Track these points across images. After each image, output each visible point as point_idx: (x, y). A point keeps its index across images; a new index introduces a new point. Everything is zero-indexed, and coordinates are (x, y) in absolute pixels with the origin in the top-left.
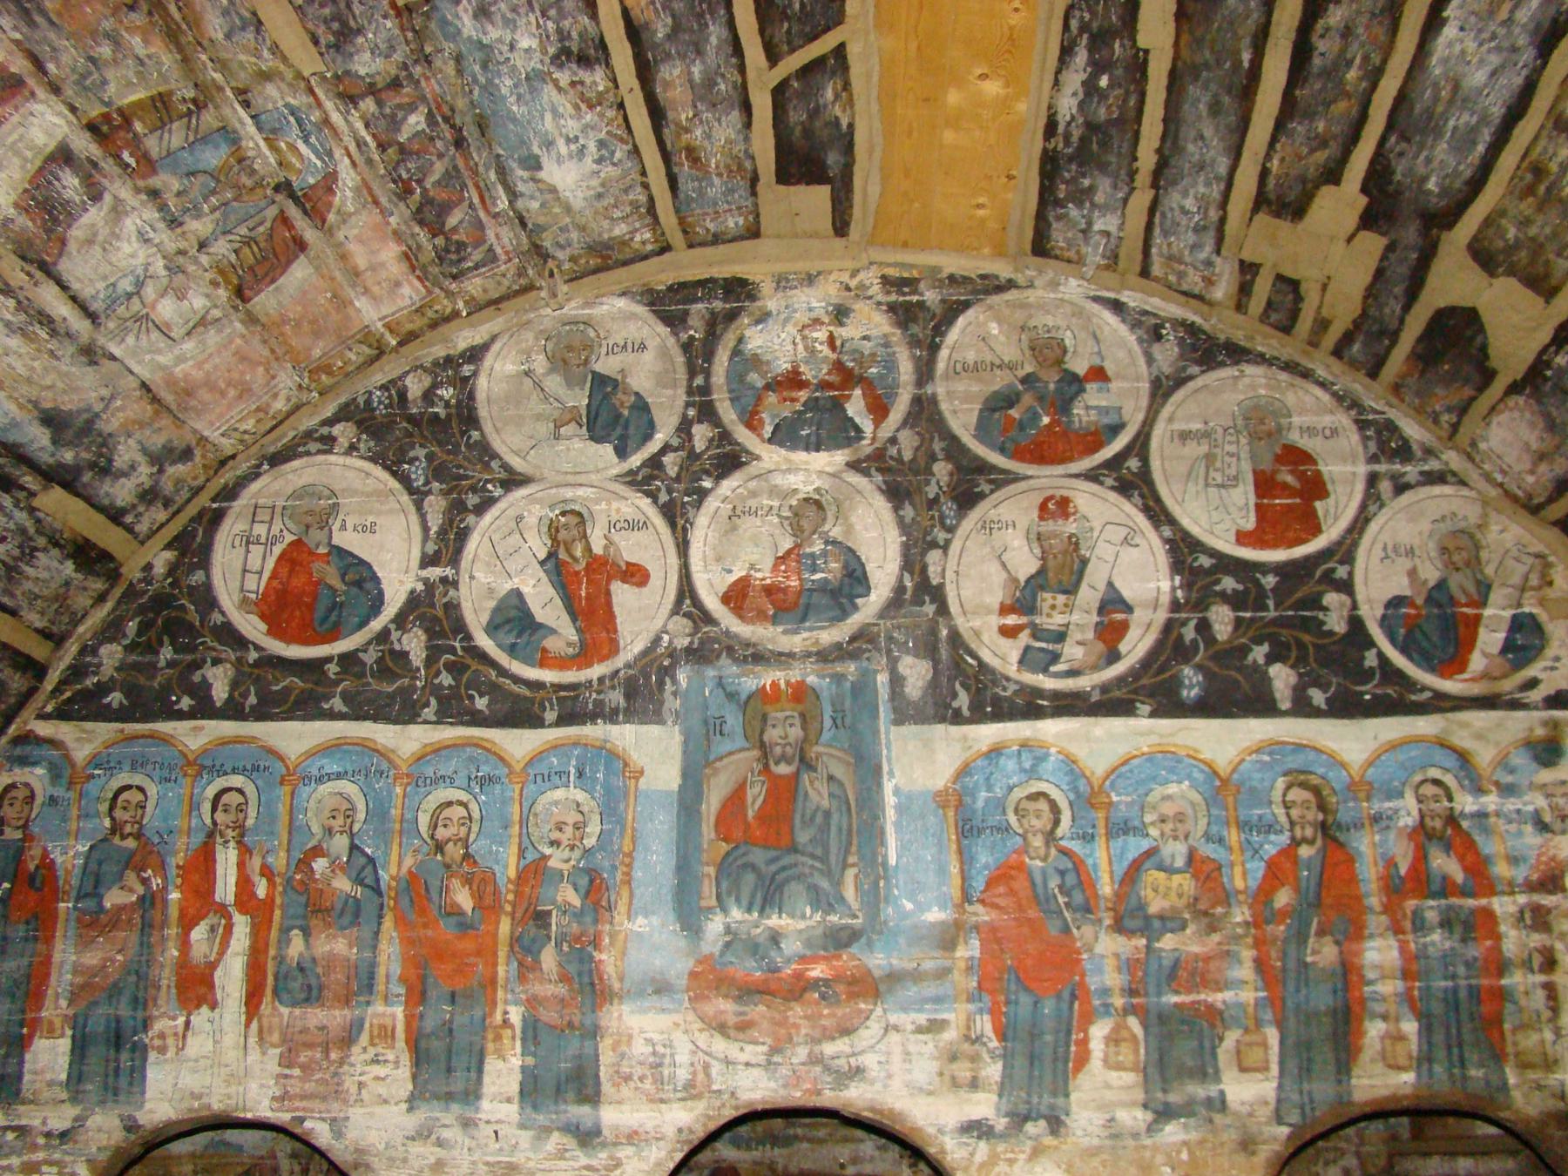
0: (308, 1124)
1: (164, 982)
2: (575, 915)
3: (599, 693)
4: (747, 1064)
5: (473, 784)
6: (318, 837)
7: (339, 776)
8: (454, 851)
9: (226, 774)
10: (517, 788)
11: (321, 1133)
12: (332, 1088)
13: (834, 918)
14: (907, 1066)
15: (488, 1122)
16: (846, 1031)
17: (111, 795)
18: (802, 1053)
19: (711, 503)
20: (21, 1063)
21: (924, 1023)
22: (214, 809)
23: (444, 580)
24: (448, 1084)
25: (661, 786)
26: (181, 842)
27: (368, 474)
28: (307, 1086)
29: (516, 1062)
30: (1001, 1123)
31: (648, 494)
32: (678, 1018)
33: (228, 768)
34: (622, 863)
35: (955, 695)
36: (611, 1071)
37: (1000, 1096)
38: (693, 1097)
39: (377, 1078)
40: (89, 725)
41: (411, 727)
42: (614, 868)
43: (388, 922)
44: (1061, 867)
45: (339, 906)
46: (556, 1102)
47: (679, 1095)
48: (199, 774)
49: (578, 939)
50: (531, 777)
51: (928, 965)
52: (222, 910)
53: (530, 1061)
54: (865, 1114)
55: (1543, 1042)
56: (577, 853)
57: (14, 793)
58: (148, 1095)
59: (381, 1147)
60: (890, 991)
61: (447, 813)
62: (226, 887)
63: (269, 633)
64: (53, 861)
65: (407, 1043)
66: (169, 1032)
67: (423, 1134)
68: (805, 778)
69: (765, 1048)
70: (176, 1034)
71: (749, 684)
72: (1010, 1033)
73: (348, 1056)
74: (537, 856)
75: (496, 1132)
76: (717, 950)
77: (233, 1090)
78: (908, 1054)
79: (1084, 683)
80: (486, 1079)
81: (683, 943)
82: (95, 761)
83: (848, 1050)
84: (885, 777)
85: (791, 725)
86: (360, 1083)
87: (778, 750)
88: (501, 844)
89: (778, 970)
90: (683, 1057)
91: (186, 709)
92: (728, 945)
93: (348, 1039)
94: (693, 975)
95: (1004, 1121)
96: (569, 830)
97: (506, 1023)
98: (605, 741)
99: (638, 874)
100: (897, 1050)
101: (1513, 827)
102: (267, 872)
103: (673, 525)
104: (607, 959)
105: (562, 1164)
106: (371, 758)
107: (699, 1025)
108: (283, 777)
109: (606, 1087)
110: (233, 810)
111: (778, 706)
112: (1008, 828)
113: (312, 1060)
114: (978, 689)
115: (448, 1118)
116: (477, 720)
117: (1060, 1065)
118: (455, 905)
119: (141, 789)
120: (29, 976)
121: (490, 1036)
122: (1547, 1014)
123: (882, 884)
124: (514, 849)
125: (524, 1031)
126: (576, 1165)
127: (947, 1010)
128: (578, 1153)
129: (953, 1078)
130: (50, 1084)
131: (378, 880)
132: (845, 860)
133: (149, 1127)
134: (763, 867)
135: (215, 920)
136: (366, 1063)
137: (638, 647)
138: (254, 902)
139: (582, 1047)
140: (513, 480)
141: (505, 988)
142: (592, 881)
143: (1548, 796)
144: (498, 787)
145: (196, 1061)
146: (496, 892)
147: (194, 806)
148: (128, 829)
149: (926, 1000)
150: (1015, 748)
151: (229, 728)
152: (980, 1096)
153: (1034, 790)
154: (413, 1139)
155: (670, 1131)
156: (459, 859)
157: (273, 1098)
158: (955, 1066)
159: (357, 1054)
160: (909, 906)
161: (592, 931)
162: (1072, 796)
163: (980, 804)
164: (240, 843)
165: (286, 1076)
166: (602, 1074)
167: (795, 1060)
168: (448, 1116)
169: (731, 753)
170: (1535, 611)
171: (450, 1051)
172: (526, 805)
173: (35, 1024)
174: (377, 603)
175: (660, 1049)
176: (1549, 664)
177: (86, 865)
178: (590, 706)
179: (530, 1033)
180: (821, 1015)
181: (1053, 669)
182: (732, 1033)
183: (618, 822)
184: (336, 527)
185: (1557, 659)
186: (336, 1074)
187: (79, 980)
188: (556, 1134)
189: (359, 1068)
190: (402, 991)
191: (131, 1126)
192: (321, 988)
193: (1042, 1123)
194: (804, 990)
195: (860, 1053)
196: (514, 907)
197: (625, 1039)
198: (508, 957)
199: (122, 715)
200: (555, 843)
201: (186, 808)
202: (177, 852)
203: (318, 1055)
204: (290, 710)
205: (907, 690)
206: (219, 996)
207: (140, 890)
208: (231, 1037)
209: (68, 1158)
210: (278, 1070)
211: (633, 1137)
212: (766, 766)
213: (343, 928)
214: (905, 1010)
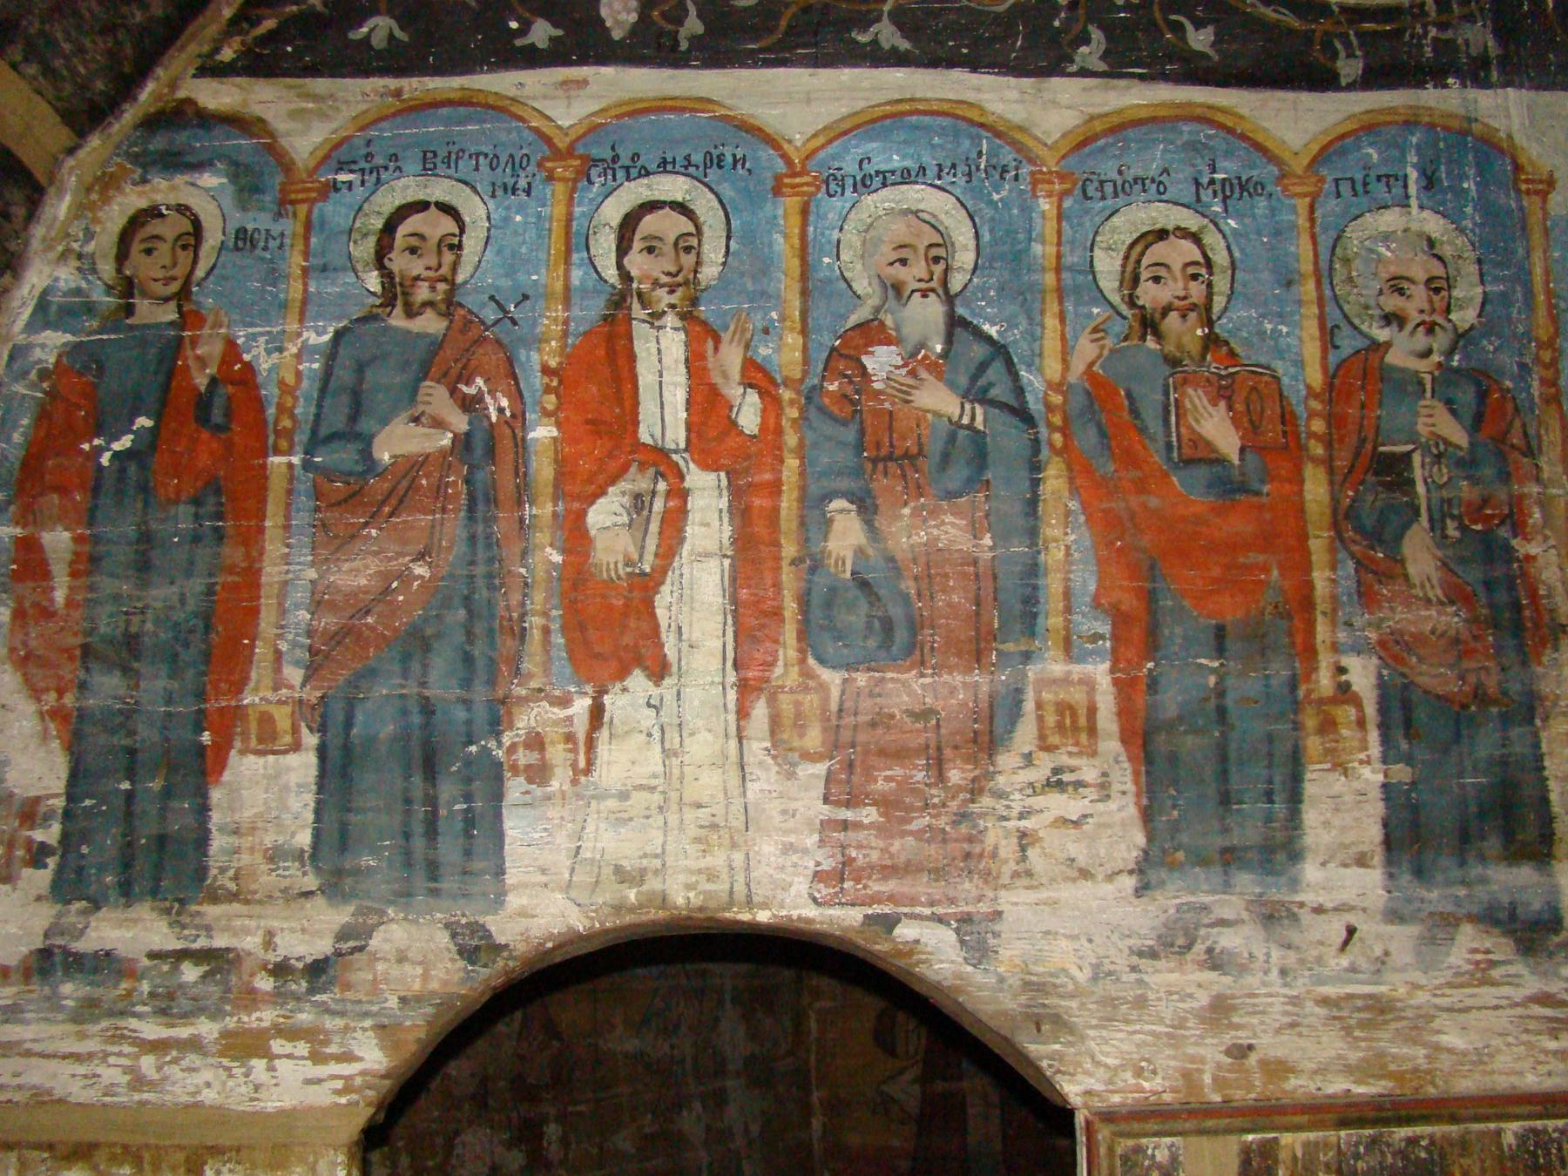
0: (906, 932)
1: (535, 621)
2: (1459, 463)
3: (1442, 26)
5: (1206, 196)
6: (875, 301)
7: (906, 177)
8: (1184, 332)
9: (648, 174)
10: (1302, 204)
12: (956, 848)
15: (1319, 910)
17: (378, 224)
20: (204, 809)
22: (623, 248)
24: (1226, 830)
26: (549, 320)
28: (896, 845)
29: (1372, 776)
33: (650, 160)
39: (1063, 822)
40: (321, 85)
41: (1056, 82)
43: (1054, 480)
45: (935, 448)
46: (1462, 864)
48: (584, 174)
49: (1477, 510)
50: (1328, 186)
52: (658, 459)
53: (1402, 773)
56: (1441, 341)
57: (155, 227)
58: (511, 878)
59: (1082, 976)
61: (1158, 251)
64: (249, 368)
65: (1124, 741)
66: (552, 733)
70: (570, 738)
73: (989, 776)
74: (1360, 343)
75: (1351, 931)
77: (717, 860)
80: (1311, 816)
82: (337, 155)
86: (1023, 835)
88: (1282, 317)
91: (542, 44)
96: (1419, 294)
97: (1344, 692)
98: (1470, 120)
102: (757, 376)
105: (1488, 994)
106: (976, 140)
108: (778, 178)
110: (668, 248)
113: (905, 785)
115: (1230, 906)
116: (1197, 72)
118: (1198, 441)
119: (448, 209)
120: (207, 619)
121: (1310, 721)
124: (1312, 327)
125: (1383, 709)
126: (1519, 994)
128: (1519, 968)
130: (275, 855)
131: (1020, 391)
133: (521, 948)
135: (643, 484)
136: (1033, 789)
138: (731, 442)
141: (1332, 616)
142: (1482, 396)
144: (1262, 204)
145: (624, 796)
146: (1287, 417)
147: (575, 241)
148: (422, 293)
154: (1153, 955)
156: (1194, 348)
157: (818, 876)
161: (1502, 495)
165: (845, 825)
171: (1223, 758)
172: (1325, 242)
173: (228, 724)
177: (328, 372)
178: (1428, 51)
179: (1397, 715)
186: (962, 816)
187: (328, 621)
188: (1467, 929)
189: (1017, 802)
190: (1105, 628)
192: (914, 626)
196: (1329, 445)
198: (1332, 550)
199: (396, 62)
200: (1392, 319)
201: (557, 244)
202: (541, 340)
203: (920, 776)
204: (781, 46)
206: (670, 650)
207: (461, 423)
208: (703, 744)
209: (331, 1023)
210: (826, 811)
213: (951, 495)
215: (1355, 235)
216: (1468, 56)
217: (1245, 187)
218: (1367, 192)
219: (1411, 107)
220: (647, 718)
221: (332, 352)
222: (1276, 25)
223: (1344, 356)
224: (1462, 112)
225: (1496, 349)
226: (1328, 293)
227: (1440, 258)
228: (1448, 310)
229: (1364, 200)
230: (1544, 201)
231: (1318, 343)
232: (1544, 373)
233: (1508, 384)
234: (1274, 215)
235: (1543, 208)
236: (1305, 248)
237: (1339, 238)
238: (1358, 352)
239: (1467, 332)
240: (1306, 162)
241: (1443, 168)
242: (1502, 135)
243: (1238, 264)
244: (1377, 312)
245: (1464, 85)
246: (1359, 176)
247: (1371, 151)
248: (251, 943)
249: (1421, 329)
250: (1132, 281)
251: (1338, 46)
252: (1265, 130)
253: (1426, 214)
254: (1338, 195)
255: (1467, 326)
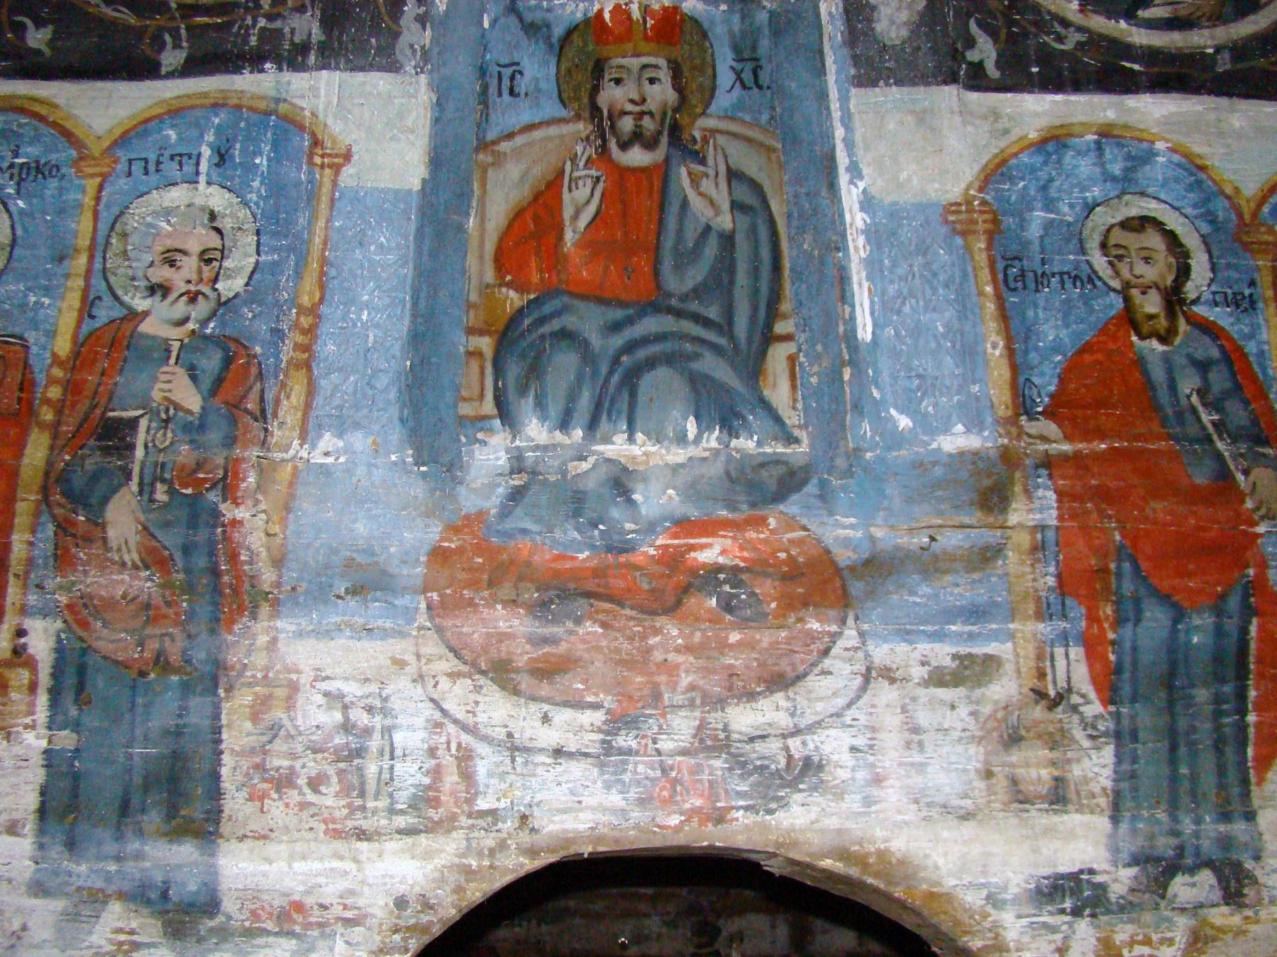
2: (187, 428)
3: (270, 17)
4: (558, 752)
13: (746, 444)
14: (917, 758)
16: (779, 681)
18: (682, 727)
21: (947, 662)
25: (386, 181)
29: (35, 742)
30: (1121, 880)
32: (401, 648)
34: (296, 326)
35: (971, 43)
36: (245, 764)
37: (1115, 819)
38: (432, 828)
42: (278, 333)
44: (1200, 354)
46: (119, 837)
47: (401, 821)
49: (189, 475)
50: (121, 167)
51: (952, 540)
53: (67, 740)
54: (827, 863)
56: (203, 308)
60: (871, 594)
68: (682, 174)
69: (598, 717)
72: (1126, 690)
74: (118, 312)
76: (492, 504)
78: (916, 730)
79: (1202, 39)
81: (419, 490)
83: (784, 720)
84: (843, 178)
85: (652, 81)
87: (627, 124)
88: (47, 290)
89: (628, 548)
90: (411, 737)
92: (516, 495)
94: (439, 555)
95: (1127, 874)
96: (189, 265)
99: (327, 348)
100: (892, 720)
107: (451, 664)
109: (235, 803)
111: (629, 47)
112: (1093, 277)
114: (1011, 35)
117: (1229, 751)
123: (847, 374)
124: (74, 299)
125: (58, 672)
127: (994, 636)
129: (1014, 782)
132: (769, 325)
134: (596, 341)
139: (182, 712)
141: (24, 578)
142: (228, 361)
144: (53, 184)
146: (27, 385)
149: (952, 614)
150: (1091, 137)
152: (1073, 820)
153: (1133, 212)
155: (378, 905)
158: (1015, 757)
160: (904, 422)
161: (220, 461)
162: (1205, 228)
163: (1034, 231)
166: (224, 771)
167: (666, 745)
169: (530, 128)
175: (360, 717)
178: (253, 41)
179: (70, 680)
180: (724, 646)
181: (1140, 13)
182: (525, 682)
183: (291, 249)
188: (116, 907)
193: (1206, 877)
194: (686, 589)
195: (812, 728)
196: (59, 413)
197: (281, 693)
198: (37, 514)
200: (159, 290)
205: (879, 27)
212: (604, 149)
214: (907, 635)
215: (139, 211)
216: (292, 43)
217: (39, 170)
218: (158, 171)
219: (223, 91)
222: (114, 22)
223: (97, 325)
224: (273, 93)
225: (254, 317)
226: (98, 265)
227: (219, 231)
228: (216, 280)
229: (153, 179)
230: (337, 173)
231: (75, 314)
232: (300, 339)
233: (258, 350)
234: (60, 196)
235: (335, 183)
236: (86, 224)
237: (122, 213)
238: (112, 321)
239: (229, 300)
240: (106, 144)
241: (238, 146)
242: (307, 113)
243: (19, 241)
244: (143, 283)
245: (280, 69)
246: (152, 157)
247: (171, 132)
249: (185, 298)
251: (168, 38)
252: (76, 117)
253: (213, 189)
254: (130, 174)
255: (231, 295)
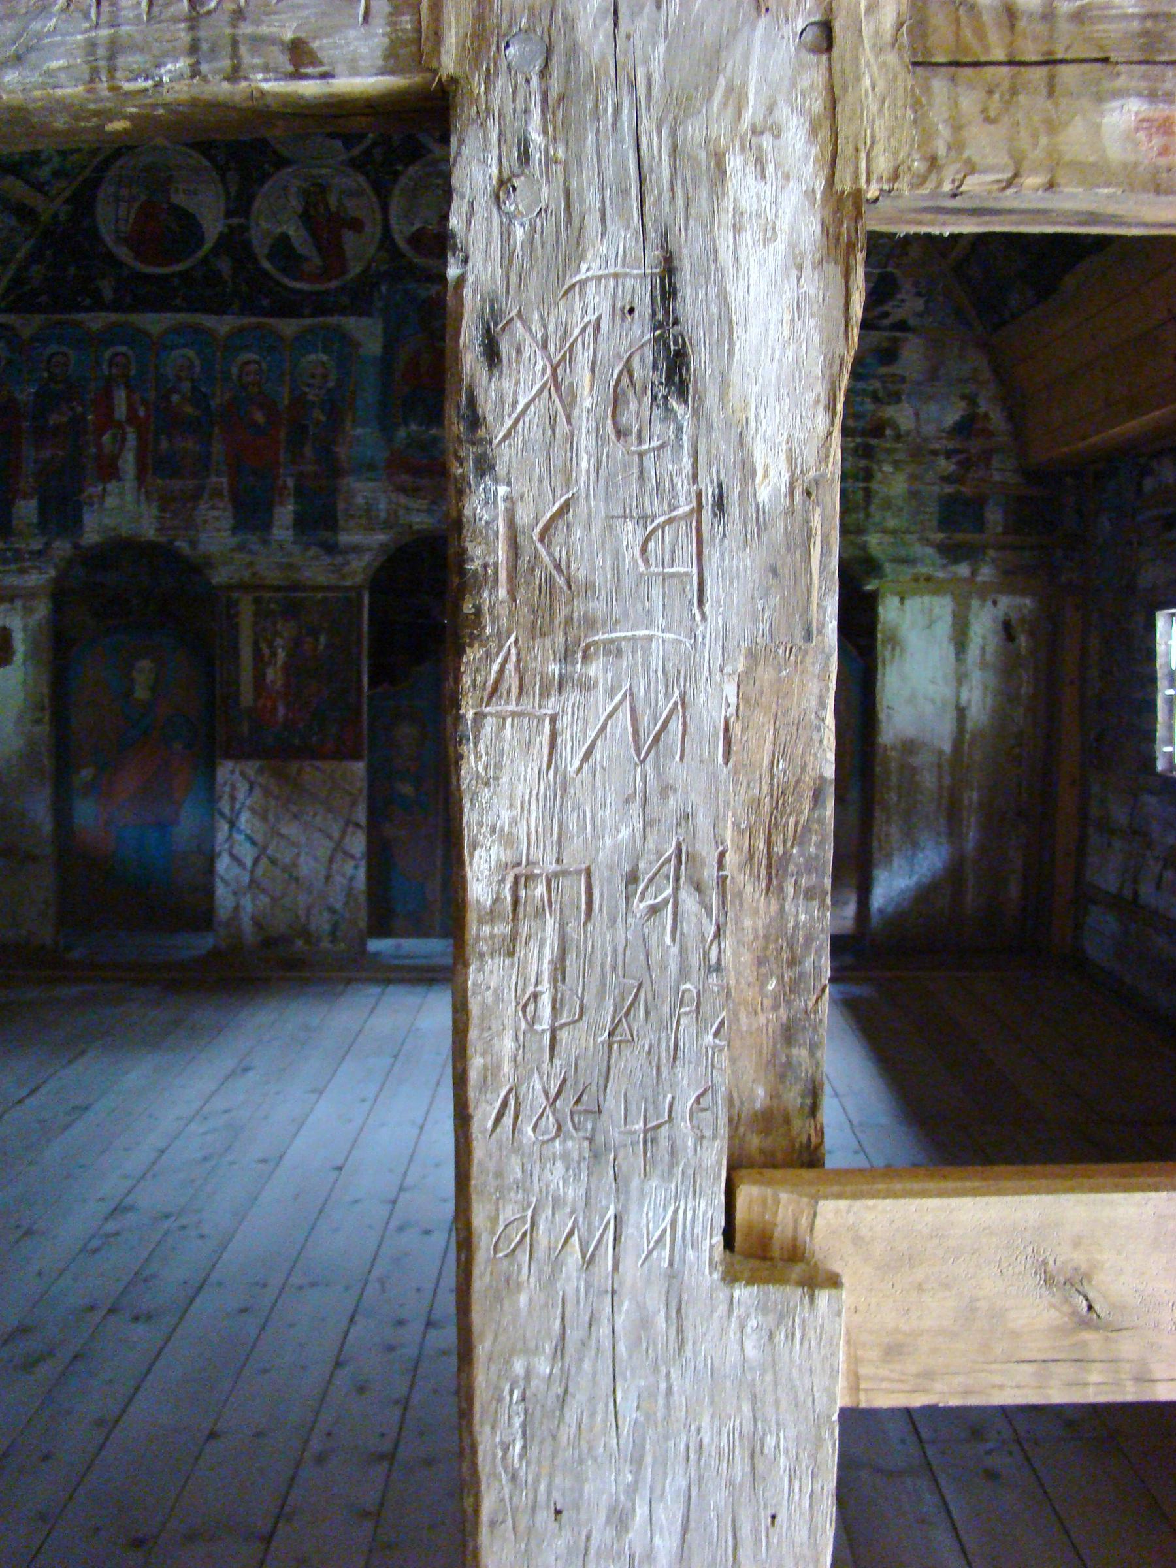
4: (418, 510)
7: (185, 346)
11: (182, 545)
19: (403, 181)
22: (110, 366)
23: (241, 226)
27: (190, 156)
29: (291, 508)
31: (362, 173)
41: (225, 317)
43: (216, 430)
52: (120, 425)
55: (858, 519)
56: (323, 391)
62: (121, 411)
63: (136, 259)
67: (241, 548)
71: (423, 294)
93: (196, 496)
97: (285, 487)
101: (858, 399)
102: (144, 402)
103: (378, 195)
104: (342, 452)
109: (341, 523)
115: (254, 538)
122: (862, 503)
130: (29, 525)
136: (208, 509)
137: (358, 270)
140: (282, 162)
143: (883, 382)
151: (114, 317)
155: (375, 546)
159: (203, 506)
164: (127, 387)
168: (253, 539)
170: (895, 271)
174: (201, 241)
175: (371, 502)
176: (896, 303)
184: (172, 191)
185: (903, 301)
191: (76, 546)
200: (309, 385)
207: (70, 413)
211: (357, 549)
220: (117, 491)
221: (36, 395)
248: (23, 546)
250: (240, 376)
